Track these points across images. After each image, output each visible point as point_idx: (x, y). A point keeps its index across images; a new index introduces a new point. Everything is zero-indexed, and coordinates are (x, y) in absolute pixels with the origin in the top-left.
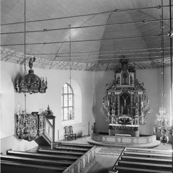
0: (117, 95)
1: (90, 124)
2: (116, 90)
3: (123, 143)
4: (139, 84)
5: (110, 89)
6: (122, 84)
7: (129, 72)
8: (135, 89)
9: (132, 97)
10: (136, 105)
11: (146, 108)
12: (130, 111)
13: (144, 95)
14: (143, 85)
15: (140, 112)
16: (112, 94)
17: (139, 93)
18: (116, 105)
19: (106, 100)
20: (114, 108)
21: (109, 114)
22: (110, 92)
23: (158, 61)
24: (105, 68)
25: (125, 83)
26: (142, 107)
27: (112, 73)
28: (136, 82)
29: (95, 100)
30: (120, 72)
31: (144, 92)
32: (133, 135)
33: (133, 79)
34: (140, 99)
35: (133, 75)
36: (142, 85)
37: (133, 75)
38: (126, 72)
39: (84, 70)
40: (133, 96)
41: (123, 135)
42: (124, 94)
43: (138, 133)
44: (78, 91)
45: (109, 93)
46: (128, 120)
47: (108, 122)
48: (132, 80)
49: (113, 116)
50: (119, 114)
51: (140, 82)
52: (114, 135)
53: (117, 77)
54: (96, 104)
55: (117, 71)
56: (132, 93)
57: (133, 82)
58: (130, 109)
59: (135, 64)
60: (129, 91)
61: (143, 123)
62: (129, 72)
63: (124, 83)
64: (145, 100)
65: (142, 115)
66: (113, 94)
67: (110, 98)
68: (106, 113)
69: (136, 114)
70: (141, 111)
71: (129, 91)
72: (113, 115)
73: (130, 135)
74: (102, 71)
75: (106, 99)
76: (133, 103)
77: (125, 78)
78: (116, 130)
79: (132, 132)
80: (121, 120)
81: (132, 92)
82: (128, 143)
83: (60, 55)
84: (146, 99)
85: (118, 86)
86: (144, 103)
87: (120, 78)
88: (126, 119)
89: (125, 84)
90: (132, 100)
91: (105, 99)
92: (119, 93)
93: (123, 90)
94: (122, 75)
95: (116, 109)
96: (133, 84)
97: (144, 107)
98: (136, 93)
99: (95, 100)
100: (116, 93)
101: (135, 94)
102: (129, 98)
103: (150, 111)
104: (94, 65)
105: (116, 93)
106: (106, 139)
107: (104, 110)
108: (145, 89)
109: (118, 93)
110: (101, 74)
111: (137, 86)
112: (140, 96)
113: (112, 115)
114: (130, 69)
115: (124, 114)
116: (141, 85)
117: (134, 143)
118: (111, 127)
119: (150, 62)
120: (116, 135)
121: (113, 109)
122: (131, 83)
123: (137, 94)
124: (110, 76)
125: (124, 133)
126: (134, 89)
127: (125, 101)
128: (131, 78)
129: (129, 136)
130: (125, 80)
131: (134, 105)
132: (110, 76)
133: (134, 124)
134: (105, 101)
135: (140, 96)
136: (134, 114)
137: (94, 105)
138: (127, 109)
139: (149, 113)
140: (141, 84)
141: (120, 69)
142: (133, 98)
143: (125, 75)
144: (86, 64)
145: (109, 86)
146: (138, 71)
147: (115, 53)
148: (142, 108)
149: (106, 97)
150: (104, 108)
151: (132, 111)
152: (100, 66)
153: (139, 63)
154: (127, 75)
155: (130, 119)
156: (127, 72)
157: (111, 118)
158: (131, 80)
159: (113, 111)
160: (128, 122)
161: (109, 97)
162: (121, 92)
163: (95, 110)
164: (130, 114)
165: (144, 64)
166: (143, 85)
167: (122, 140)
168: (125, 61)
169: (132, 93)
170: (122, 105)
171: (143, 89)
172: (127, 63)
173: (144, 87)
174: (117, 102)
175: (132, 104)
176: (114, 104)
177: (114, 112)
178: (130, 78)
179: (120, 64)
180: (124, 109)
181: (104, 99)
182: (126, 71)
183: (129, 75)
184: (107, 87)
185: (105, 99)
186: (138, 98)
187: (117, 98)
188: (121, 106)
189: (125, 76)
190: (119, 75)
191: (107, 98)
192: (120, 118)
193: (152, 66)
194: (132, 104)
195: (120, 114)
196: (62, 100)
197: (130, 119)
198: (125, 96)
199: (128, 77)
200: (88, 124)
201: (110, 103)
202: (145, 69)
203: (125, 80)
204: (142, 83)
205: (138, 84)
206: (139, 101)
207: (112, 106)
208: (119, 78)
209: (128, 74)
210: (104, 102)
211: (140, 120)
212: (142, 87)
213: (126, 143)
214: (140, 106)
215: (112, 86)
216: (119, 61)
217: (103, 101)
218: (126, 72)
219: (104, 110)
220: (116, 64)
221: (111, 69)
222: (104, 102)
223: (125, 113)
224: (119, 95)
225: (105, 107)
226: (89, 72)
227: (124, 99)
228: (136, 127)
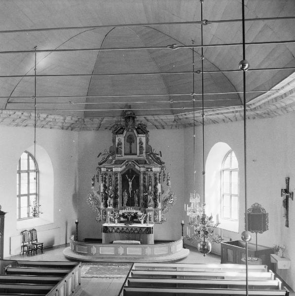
0: (116, 173)
1: (68, 224)
2: (115, 163)
3: (127, 255)
4: (155, 155)
5: (104, 162)
6: (125, 154)
7: (138, 133)
8: (148, 162)
9: (142, 177)
10: (149, 189)
11: (166, 195)
12: (139, 200)
13: (162, 173)
14: (161, 156)
17: (154, 169)
18: (116, 190)
19: (98, 181)
20: (112, 196)
21: (102, 207)
22: (104, 167)
23: (185, 117)
24: (96, 126)
25: (131, 151)
26: (158, 194)
27: (109, 134)
28: (149, 151)
29: (77, 181)
31: (162, 168)
32: (144, 242)
33: (144, 146)
34: (156, 179)
36: (159, 156)
37: (144, 140)
38: (131, 133)
39: (58, 128)
40: (144, 173)
41: (128, 242)
43: (151, 238)
44: (47, 167)
45: (103, 169)
46: (135, 216)
47: (100, 221)
48: (142, 147)
49: (109, 210)
50: (119, 205)
51: (156, 150)
52: (112, 243)
53: (117, 141)
54: (79, 188)
55: (118, 131)
56: (142, 169)
57: (144, 151)
59: (147, 120)
60: (137, 167)
61: (160, 220)
62: (138, 133)
63: (128, 151)
64: (164, 180)
65: (160, 206)
66: (109, 170)
67: (105, 178)
68: (98, 204)
70: (158, 200)
72: (111, 207)
73: (139, 242)
74: (90, 130)
75: (98, 179)
76: (144, 186)
77: (131, 144)
78: (115, 234)
79: (141, 236)
80: (123, 216)
81: (142, 167)
82: (138, 255)
83: (16, 100)
84: (166, 179)
85: (118, 157)
86: (161, 186)
87: (121, 143)
88: (133, 215)
89: (131, 153)
90: (142, 182)
91: (96, 180)
92: (119, 169)
95: (116, 197)
96: (144, 154)
97: (163, 192)
98: (149, 170)
99: (77, 181)
100: (114, 170)
101: (148, 171)
102: (138, 178)
103: (172, 199)
104: (77, 119)
105: (114, 170)
106: (98, 250)
107: (94, 199)
108: (164, 163)
109: (118, 169)
110: (89, 136)
111: (150, 158)
112: (155, 174)
113: (108, 207)
114: (138, 128)
115: (128, 204)
116: (157, 156)
117: (146, 255)
118: (106, 229)
119: (172, 117)
120: (114, 242)
121: (110, 197)
122: (141, 153)
123: (152, 170)
124: (105, 140)
125: (129, 239)
126: (145, 163)
127: (130, 183)
128: (141, 143)
129: (138, 244)
130: (131, 148)
131: (146, 189)
132: (105, 140)
133: (145, 222)
134: (96, 183)
135: (155, 174)
136: (146, 205)
137: (75, 189)
138: (133, 197)
140: (158, 155)
141: (122, 128)
143: (131, 139)
144: (62, 118)
145: (103, 156)
146: (152, 133)
147: (114, 100)
149: (97, 176)
150: (95, 196)
151: (142, 201)
152: (87, 122)
153: (153, 118)
154: (135, 139)
155: (140, 213)
157: (105, 213)
158: (141, 147)
159: (110, 201)
160: (135, 220)
161: (102, 176)
162: (124, 167)
163: (77, 198)
164: (139, 206)
165: (162, 120)
166: (161, 156)
167: (125, 250)
168: (131, 114)
169: (142, 169)
171: (161, 163)
172: (134, 118)
173: (162, 159)
174: (117, 185)
175: (142, 188)
176: (111, 188)
177: (112, 202)
178: (140, 143)
179: (123, 120)
180: (129, 197)
181: (93, 180)
183: (138, 138)
184: (100, 159)
185: (96, 180)
186: (153, 178)
187: (117, 178)
188: (123, 191)
189: (130, 140)
190: (121, 138)
191: (100, 178)
192: (121, 212)
193: (175, 123)
194: (142, 188)
195: (123, 205)
196: (18, 182)
197: (140, 213)
198: (131, 175)
199: (135, 141)
200: (65, 224)
201: (105, 186)
202: (164, 128)
203: (131, 148)
205: (152, 153)
206: (153, 184)
207: (108, 192)
208: (120, 144)
209: (136, 136)
210: (93, 185)
211: (155, 214)
212: (158, 158)
213: (134, 255)
214: (156, 192)
215: (108, 157)
216: (120, 114)
217: (92, 182)
218: (131, 133)
219: (94, 199)
220: (115, 119)
221: (106, 128)
222: (93, 185)
223: (131, 203)
225: (96, 194)
226: (69, 132)
227: (129, 180)
228: (150, 228)
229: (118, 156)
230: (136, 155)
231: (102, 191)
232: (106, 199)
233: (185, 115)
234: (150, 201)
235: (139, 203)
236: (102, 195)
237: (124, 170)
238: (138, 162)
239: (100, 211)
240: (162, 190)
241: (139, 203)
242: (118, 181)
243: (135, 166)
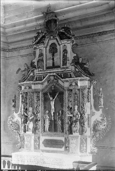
0: (37, 92)
2: (36, 80)
6: (48, 68)
17: (80, 84)
25: (53, 63)
35: (68, 45)
53: (38, 52)
56: (66, 85)
62: (61, 39)
70: (86, 123)
71: (60, 82)
72: (30, 133)
77: (53, 55)
89: (54, 66)
92: (39, 87)
100: (33, 87)
112: (83, 89)
122: (64, 63)
127: (52, 104)
159: (31, 125)
164: (63, 131)
180: (50, 120)
188: (45, 113)
190: (44, 49)
208: (41, 55)
224: (42, 90)
227: (51, 99)
230: (59, 67)
237: (47, 86)
238: (61, 76)
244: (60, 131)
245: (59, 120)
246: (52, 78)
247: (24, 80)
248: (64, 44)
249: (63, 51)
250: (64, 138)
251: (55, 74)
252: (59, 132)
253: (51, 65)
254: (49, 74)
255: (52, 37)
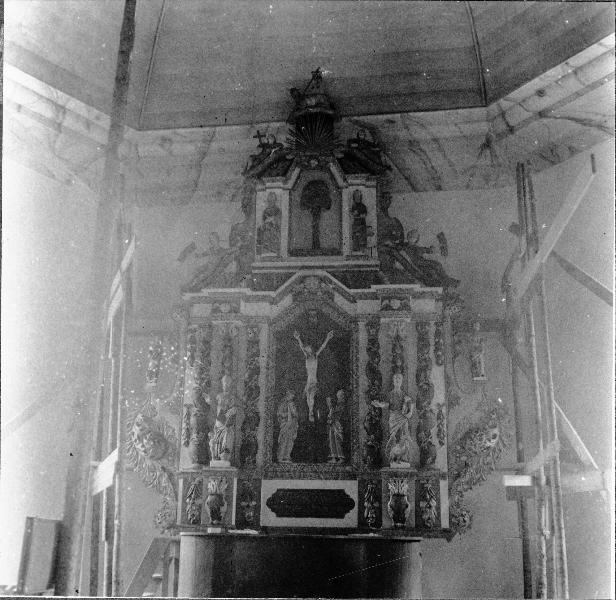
0: (252, 324)
4: (415, 251)
6: (293, 253)
9: (362, 337)
10: (391, 386)
14: (444, 250)
15: (419, 442)
16: (215, 310)
17: (417, 305)
25: (316, 244)
26: (433, 407)
30: (284, 174)
31: (447, 300)
33: (372, 218)
34: (422, 342)
36: (436, 256)
37: (370, 197)
38: (317, 175)
40: (373, 324)
42: (306, 316)
53: (261, 205)
57: (373, 240)
58: (346, 424)
60: (339, 299)
61: (445, 523)
63: (303, 240)
69: (396, 450)
71: (339, 299)
76: (373, 371)
77: (316, 216)
81: (366, 297)
86: (447, 378)
89: (316, 248)
92: (265, 309)
93: (299, 287)
94: (300, 190)
97: (452, 402)
103: (496, 431)
105: (246, 309)
113: (213, 463)
121: (222, 418)
123: (405, 307)
127: (312, 366)
128: (359, 208)
130: (316, 228)
139: (492, 443)
142: (373, 341)
148: (439, 417)
156: (333, 177)
162: (288, 301)
170: (291, 396)
174: (256, 371)
180: (303, 423)
182: (323, 167)
183: (347, 194)
203: (316, 228)
204: (437, 244)
205: (403, 245)
206: (412, 369)
208: (273, 211)
212: (434, 265)
214: (426, 391)
218: (326, 176)
229: (263, 260)
230: (338, 252)
231: (189, 396)
232: (205, 428)
233: (540, 93)
234: (398, 436)
235: (347, 449)
236: (188, 415)
237: (288, 311)
239: (175, 485)
240: (448, 392)
241: (347, 449)
242: (257, 354)
243: (332, 298)
244: (337, 459)
245: (337, 423)
246: (312, 284)
247: (208, 282)
248: (355, 188)
249: (352, 210)
250: (356, 482)
251: (319, 272)
252: (334, 461)
253: (308, 244)
254: (300, 273)
255: (314, 163)
